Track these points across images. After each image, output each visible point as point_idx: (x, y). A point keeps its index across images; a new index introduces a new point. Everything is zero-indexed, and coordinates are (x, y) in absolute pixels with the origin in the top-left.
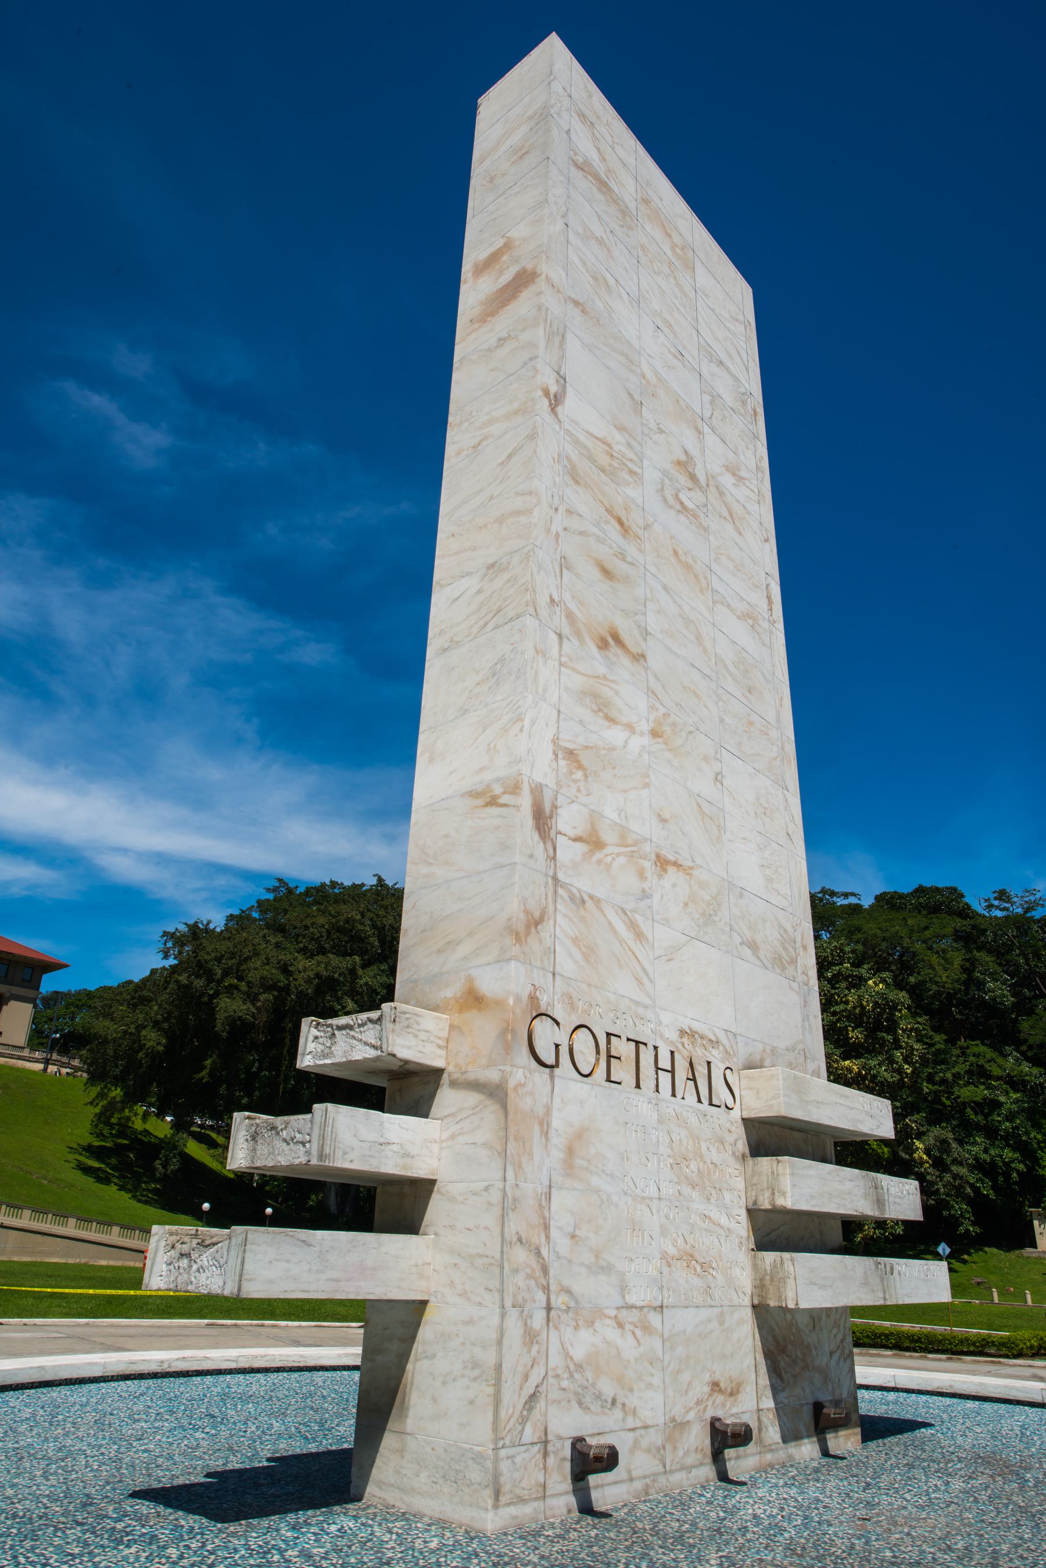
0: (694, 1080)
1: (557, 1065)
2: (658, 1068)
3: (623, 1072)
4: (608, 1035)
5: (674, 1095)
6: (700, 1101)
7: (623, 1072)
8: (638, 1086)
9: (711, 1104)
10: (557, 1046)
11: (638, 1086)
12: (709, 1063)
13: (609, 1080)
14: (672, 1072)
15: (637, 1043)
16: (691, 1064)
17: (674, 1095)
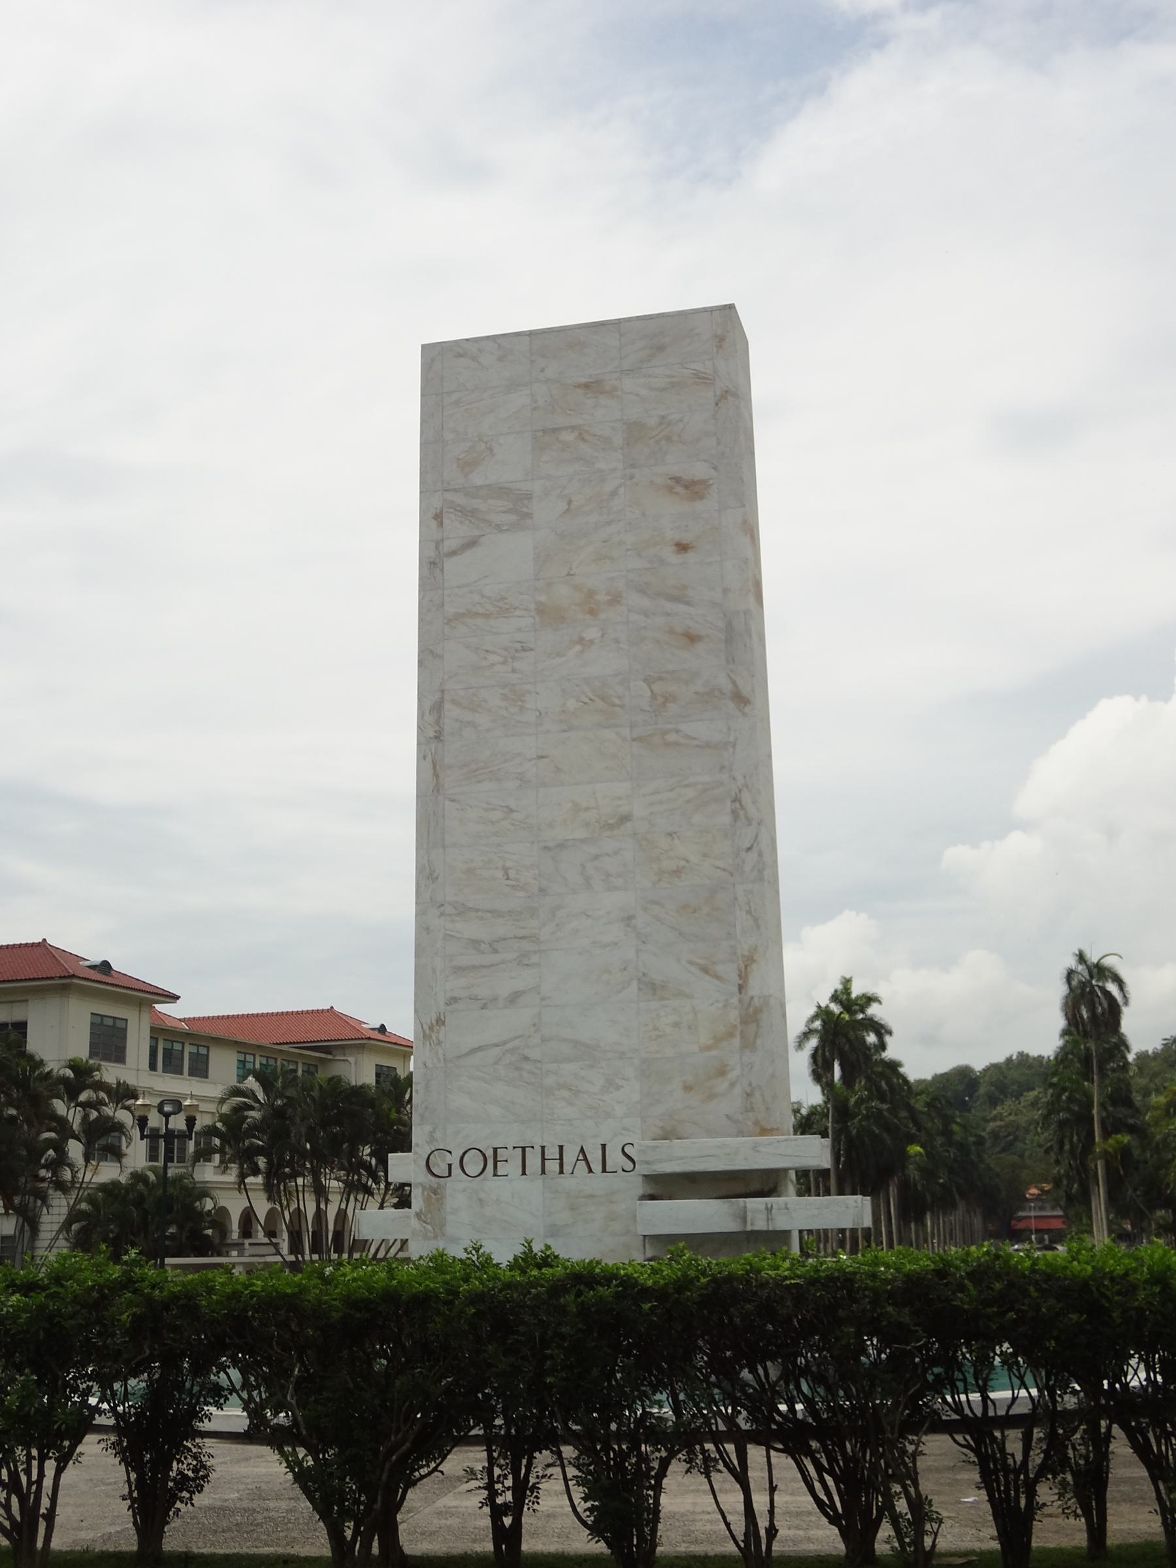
0: (586, 1159)
1: (450, 1175)
2: (543, 1159)
3: (511, 1168)
4: (495, 1150)
5: (561, 1172)
6: (590, 1171)
7: (511, 1168)
8: (524, 1173)
9: (604, 1170)
10: (450, 1165)
11: (524, 1173)
12: (604, 1146)
13: (495, 1175)
14: (561, 1159)
15: (524, 1149)
16: (582, 1150)
17: (561, 1172)
